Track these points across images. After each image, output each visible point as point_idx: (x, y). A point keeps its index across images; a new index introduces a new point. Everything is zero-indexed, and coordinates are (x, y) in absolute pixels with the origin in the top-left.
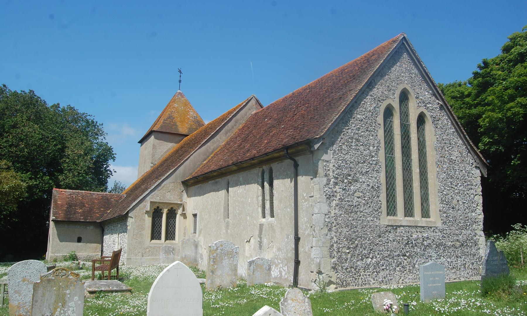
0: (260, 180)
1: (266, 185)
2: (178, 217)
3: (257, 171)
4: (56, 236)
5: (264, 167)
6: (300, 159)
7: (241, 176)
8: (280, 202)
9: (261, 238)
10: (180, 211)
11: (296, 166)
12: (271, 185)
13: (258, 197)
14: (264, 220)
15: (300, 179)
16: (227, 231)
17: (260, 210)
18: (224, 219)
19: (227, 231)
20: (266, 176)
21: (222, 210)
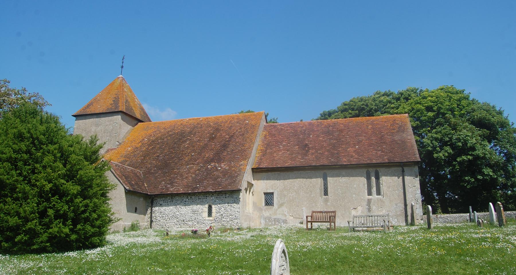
0: (365, 175)
1: (373, 179)
2: (251, 193)
3: (365, 171)
4: (125, 205)
5: (371, 170)
6: (406, 169)
7: (344, 172)
8: (389, 187)
9: (369, 206)
10: (252, 191)
11: (403, 171)
12: (377, 178)
13: (364, 185)
14: (370, 197)
15: (406, 178)
16: (326, 204)
17: (366, 191)
18: (321, 196)
19: (326, 204)
20: (373, 173)
21: (318, 191)
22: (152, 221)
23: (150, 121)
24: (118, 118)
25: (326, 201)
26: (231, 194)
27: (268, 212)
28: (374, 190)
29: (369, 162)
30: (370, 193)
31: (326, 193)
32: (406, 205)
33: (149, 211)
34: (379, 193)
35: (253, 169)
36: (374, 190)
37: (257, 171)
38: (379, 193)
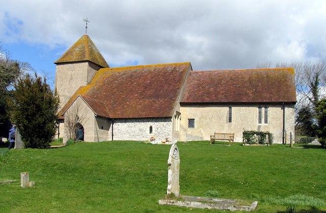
14: (260, 124)
22: (113, 135)
23: (108, 66)
24: (87, 63)
25: (230, 127)
26: (167, 119)
27: (190, 131)
28: (263, 120)
29: (261, 101)
30: (260, 122)
31: (230, 120)
32: (284, 131)
33: (111, 129)
34: (266, 122)
35: (181, 103)
36: (263, 120)
37: (183, 104)
38: (266, 122)
